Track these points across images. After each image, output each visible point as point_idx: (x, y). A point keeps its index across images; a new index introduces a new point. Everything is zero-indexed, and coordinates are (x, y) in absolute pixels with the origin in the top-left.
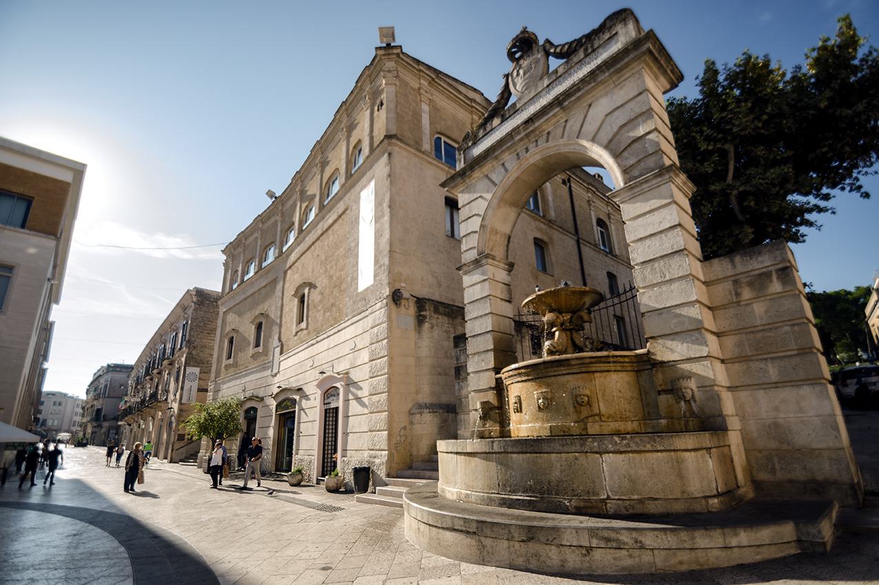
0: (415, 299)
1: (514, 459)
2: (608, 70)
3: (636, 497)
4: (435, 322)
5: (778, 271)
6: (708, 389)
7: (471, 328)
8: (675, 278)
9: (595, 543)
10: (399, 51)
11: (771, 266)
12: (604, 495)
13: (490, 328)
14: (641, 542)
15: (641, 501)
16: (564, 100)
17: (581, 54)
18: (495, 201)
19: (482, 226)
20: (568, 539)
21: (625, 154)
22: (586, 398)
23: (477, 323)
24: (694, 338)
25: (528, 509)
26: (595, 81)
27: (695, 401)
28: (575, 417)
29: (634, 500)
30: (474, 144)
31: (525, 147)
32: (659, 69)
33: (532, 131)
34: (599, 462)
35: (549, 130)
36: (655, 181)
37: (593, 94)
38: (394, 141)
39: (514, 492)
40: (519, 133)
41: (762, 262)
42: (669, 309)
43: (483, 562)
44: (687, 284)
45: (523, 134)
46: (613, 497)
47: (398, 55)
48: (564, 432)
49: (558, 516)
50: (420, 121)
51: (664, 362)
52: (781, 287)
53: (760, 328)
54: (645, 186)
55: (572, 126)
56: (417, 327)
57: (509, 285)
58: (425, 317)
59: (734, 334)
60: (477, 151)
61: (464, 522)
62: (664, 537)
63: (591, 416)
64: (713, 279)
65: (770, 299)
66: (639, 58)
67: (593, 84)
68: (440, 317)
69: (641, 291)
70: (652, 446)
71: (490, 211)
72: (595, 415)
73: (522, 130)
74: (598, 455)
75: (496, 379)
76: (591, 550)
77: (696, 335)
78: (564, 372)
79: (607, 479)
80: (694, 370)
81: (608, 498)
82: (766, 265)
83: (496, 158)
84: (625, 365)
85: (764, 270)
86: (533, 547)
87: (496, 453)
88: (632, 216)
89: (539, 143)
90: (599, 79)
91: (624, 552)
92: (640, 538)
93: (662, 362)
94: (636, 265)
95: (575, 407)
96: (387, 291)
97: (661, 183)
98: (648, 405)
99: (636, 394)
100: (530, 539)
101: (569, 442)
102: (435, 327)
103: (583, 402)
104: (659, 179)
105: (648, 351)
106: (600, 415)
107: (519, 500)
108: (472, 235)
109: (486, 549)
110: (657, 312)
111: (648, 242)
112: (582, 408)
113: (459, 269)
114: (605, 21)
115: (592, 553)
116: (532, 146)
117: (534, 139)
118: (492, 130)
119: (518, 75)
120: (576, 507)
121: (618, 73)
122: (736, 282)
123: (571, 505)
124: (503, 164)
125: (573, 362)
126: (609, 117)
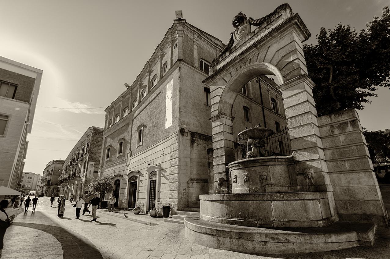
0: (191, 133)
1: (233, 203)
2: (277, 31)
3: (286, 220)
4: (199, 143)
5: (350, 121)
6: (319, 173)
7: (216, 145)
8: (305, 124)
9: (268, 240)
10: (184, 21)
11: (348, 119)
12: (272, 219)
13: (223, 146)
14: (288, 239)
15: (288, 222)
16: (258, 44)
17: (266, 24)
18: (226, 89)
19: (221, 100)
20: (256, 238)
22: (265, 177)
23: (218, 143)
24: (313, 151)
25: (239, 225)
26: (271, 37)
27: (313, 179)
28: (260, 185)
29: (285, 221)
30: (217, 64)
31: (240, 65)
32: (300, 31)
33: (243, 58)
34: (271, 205)
35: (251, 58)
36: (297, 81)
37: (270, 42)
38: (182, 62)
39: (233, 217)
40: (237, 59)
41: (344, 118)
42: (302, 138)
43: (219, 248)
44: (310, 127)
45: (239, 60)
46: (276, 220)
47: (184, 23)
48: (255, 191)
49: (252, 228)
50: (193, 53)
51: (300, 161)
52: (352, 129)
53: (342, 147)
54: (293, 83)
55: (261, 56)
57: (232, 127)
58: (195, 140)
59: (331, 149)
60: (219, 67)
61: (211, 230)
62: (298, 238)
63: (267, 185)
64: (322, 125)
65: (347, 134)
66: (291, 26)
67: (271, 38)
68: (201, 140)
69: (290, 130)
70: (294, 198)
71: (224, 94)
72: (269, 184)
73: (239, 58)
74: (270, 202)
75: (226, 168)
76: (266, 243)
77: (314, 150)
78: (256, 165)
79: (274, 212)
80: (313, 165)
81: (274, 220)
82: (346, 119)
83: (227, 70)
84: (282, 162)
85: (345, 121)
86: (241, 241)
87: (225, 200)
88: (287, 97)
90: (273, 36)
91: (281, 244)
92: (288, 238)
93: (299, 161)
94: (288, 118)
95: (260, 181)
96: (178, 129)
97: (300, 82)
98: (292, 180)
99: (287, 175)
100: (240, 238)
101: (257, 196)
102: (199, 145)
103: (264, 178)
104: (299, 81)
105: (293, 156)
106: (271, 184)
107: (235, 221)
108: (216, 104)
109: (220, 242)
110: (296, 139)
111: (293, 108)
112: (263, 181)
113: (210, 119)
114: (276, 9)
115: (267, 244)
116: (243, 65)
117: (244, 62)
118: (225, 57)
119: (237, 33)
120: (260, 224)
121: (282, 33)
122: (332, 126)
123: (258, 223)
124: (230, 73)
125: (260, 161)
126: (277, 53)
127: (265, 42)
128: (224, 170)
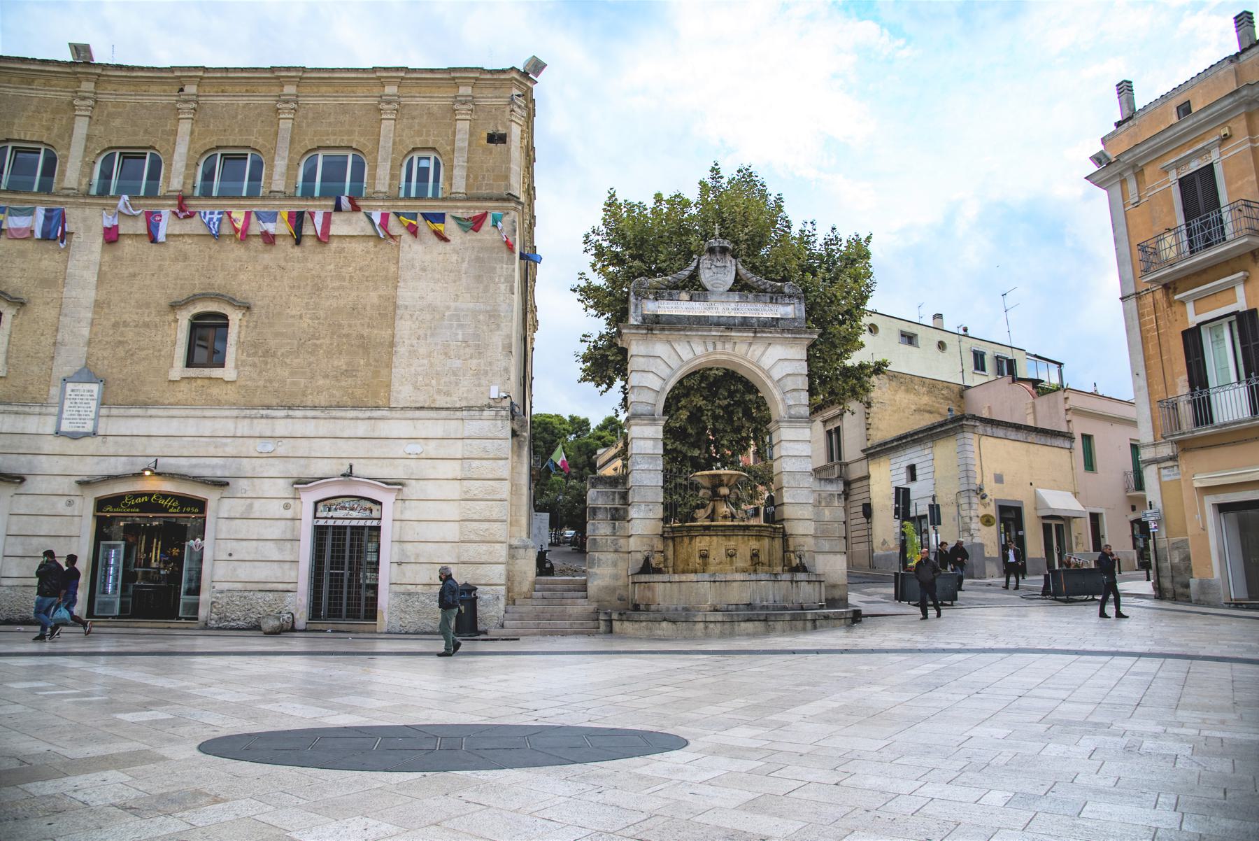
21: (788, 395)
45: (719, 334)
56: (515, 448)
75: (663, 527)
89: (726, 346)
126: (781, 363)
127: (770, 335)
128: (660, 532)
